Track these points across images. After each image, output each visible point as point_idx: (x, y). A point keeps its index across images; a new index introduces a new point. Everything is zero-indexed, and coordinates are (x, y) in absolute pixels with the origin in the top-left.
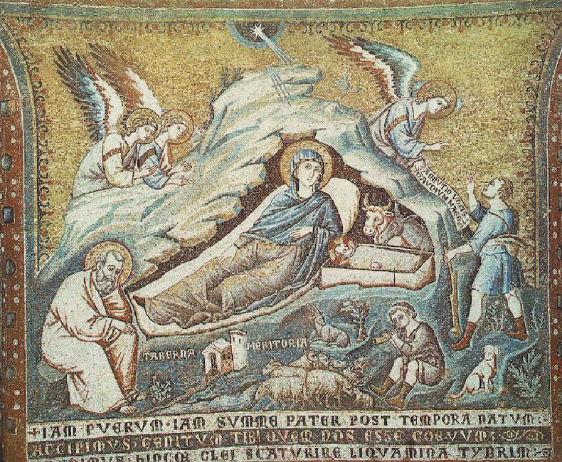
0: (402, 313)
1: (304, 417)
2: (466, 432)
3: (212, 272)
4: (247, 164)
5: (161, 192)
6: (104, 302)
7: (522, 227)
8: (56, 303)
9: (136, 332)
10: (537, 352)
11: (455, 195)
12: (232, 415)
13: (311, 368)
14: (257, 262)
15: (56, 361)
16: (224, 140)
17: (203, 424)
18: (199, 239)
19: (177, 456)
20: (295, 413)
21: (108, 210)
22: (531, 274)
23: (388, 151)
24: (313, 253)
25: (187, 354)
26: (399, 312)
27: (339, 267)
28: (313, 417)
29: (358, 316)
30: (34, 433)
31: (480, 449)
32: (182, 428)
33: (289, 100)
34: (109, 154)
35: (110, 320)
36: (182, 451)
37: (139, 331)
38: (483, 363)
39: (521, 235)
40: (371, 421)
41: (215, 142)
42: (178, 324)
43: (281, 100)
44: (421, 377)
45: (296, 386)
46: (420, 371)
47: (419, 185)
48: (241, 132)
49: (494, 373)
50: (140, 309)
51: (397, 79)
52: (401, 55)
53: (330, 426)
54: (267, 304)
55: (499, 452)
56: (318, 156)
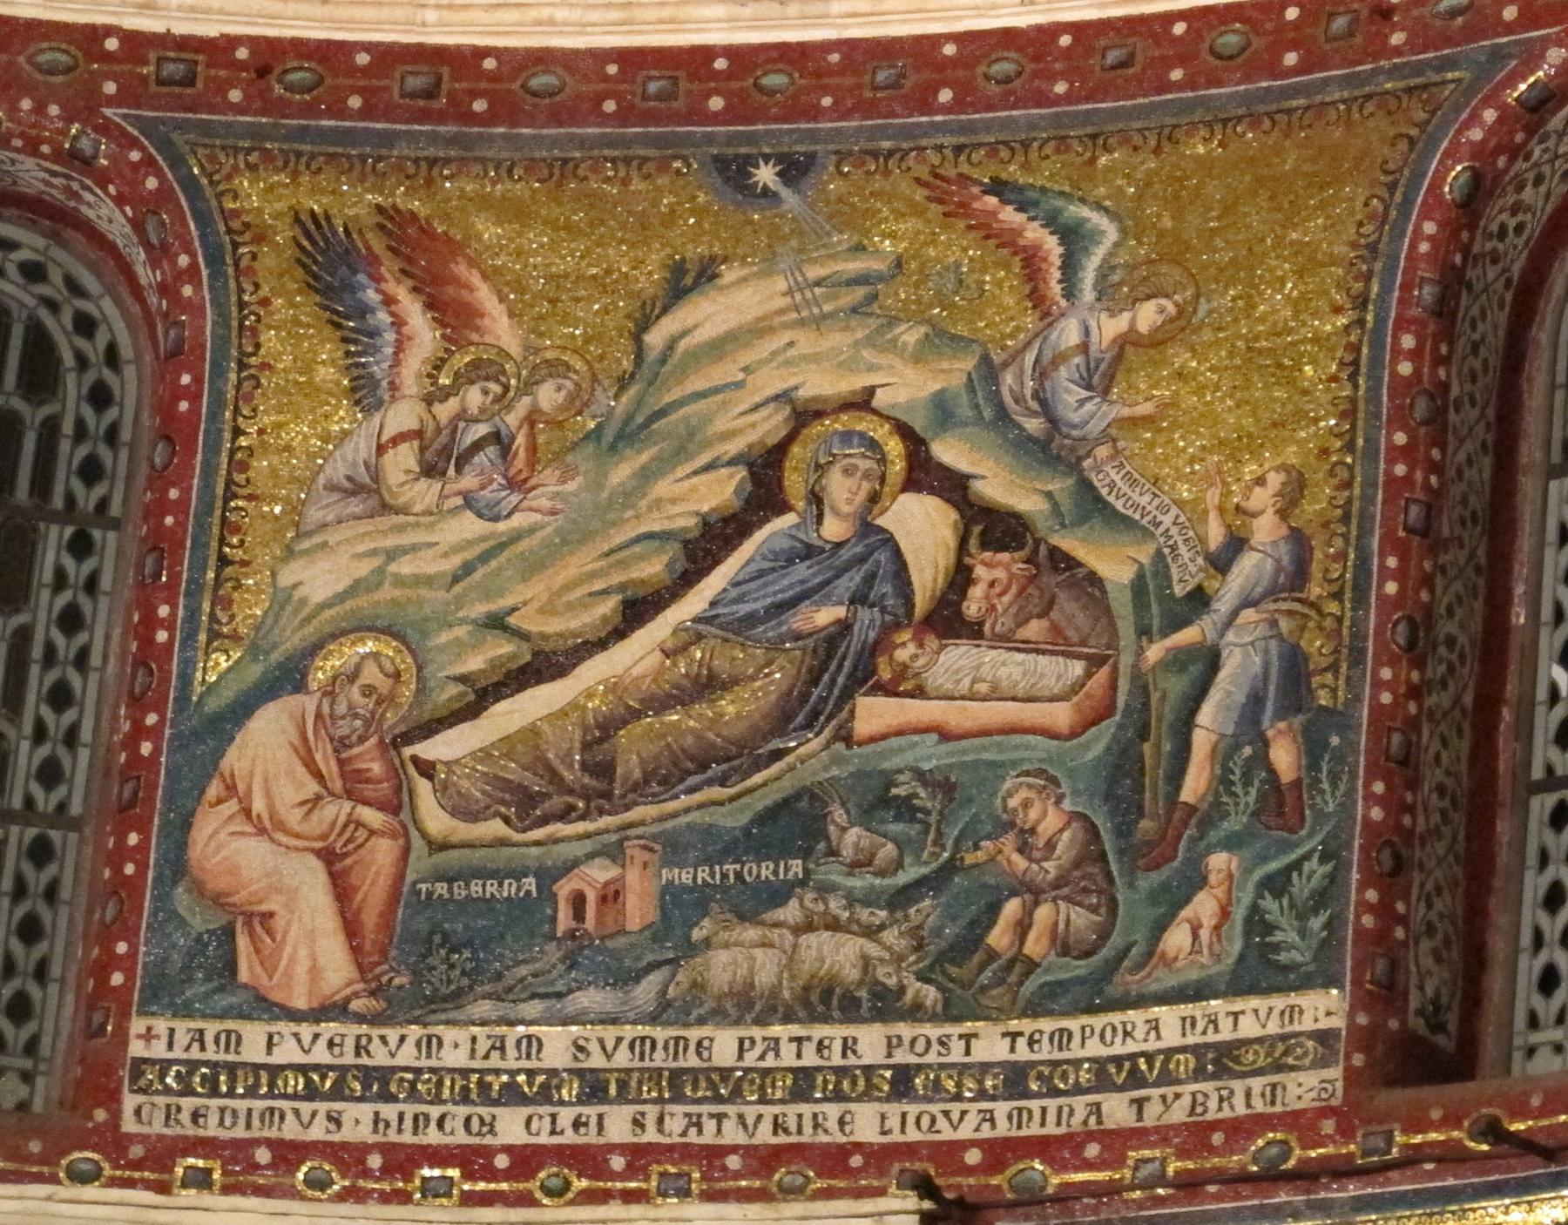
0: (1032, 794)
1: (777, 1040)
2: (1149, 1057)
4: (709, 467)
5: (502, 526)
6: (341, 763)
8: (235, 759)
9: (406, 834)
10: (1323, 859)
12: (610, 1033)
13: (808, 927)
14: (707, 685)
15: (217, 883)
16: (662, 413)
17: (539, 1051)
18: (576, 636)
19: (468, 1120)
20: (757, 1032)
21: (376, 562)
22: (1329, 678)
23: (1034, 425)
24: (840, 666)
25: (519, 889)
26: (1024, 794)
27: (897, 695)
28: (799, 1040)
30: (148, 1036)
31: (1177, 1096)
32: (486, 1057)
33: (819, 322)
34: (396, 440)
35: (347, 806)
36: (483, 1111)
37: (414, 833)
38: (1201, 896)
39: (1315, 590)
40: (935, 1047)
41: (640, 419)
42: (507, 821)
43: (802, 323)
44: (1063, 945)
45: (766, 969)
46: (1061, 926)
47: (1098, 499)
49: (1225, 913)
50: (423, 786)
51: (1070, 266)
52: (1086, 212)
53: (837, 1060)
54: (723, 781)
55: (1221, 1099)
56: (873, 445)
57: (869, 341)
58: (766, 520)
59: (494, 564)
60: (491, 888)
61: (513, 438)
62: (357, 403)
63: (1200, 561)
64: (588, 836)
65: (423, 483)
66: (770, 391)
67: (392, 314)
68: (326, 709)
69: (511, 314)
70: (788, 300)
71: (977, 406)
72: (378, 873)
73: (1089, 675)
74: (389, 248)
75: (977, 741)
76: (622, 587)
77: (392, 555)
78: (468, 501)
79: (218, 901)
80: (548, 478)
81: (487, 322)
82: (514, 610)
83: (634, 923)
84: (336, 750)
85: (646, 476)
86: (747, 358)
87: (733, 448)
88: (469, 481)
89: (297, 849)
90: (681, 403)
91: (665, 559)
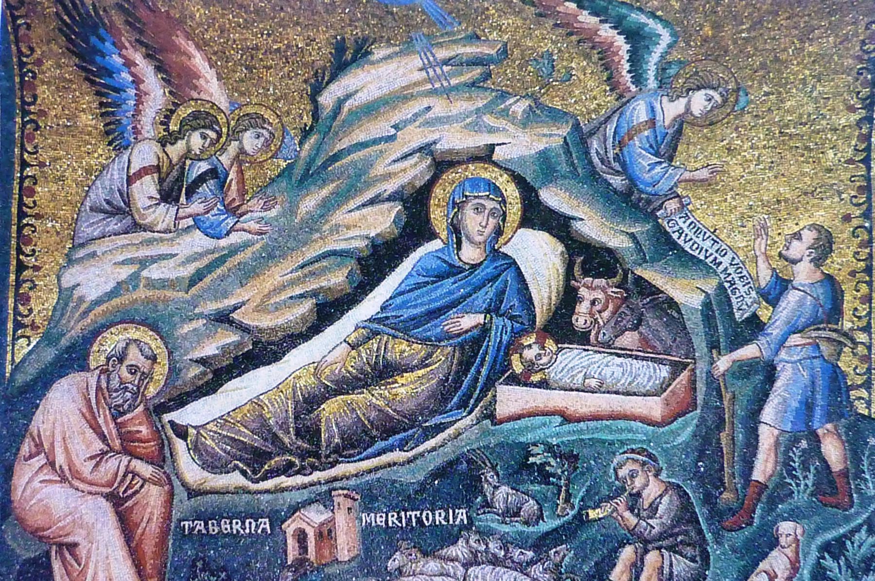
0: (636, 467)
3: (307, 381)
4: (372, 202)
5: (223, 242)
7: (848, 313)
11: (733, 258)
15: (35, 520)
16: (336, 158)
24: (483, 360)
25: (257, 527)
29: (559, 471)
33: (447, 92)
35: (125, 459)
37: (176, 483)
42: (244, 473)
46: (666, 570)
48: (363, 145)
50: (180, 445)
51: (636, 60)
56: (496, 190)
57: (488, 109)
58: (418, 245)
59: (219, 271)
60: (237, 526)
61: (227, 175)
62: (110, 144)
63: (753, 294)
64: (304, 487)
65: (163, 207)
66: (415, 145)
67: (133, 74)
68: (104, 385)
69: (219, 79)
70: (424, 74)
71: (573, 164)
72: (152, 513)
73: (674, 375)
74: (127, 22)
75: (592, 424)
76: (314, 294)
77: (144, 263)
78: (198, 223)
79: (36, 534)
80: (256, 204)
81: (202, 81)
82: (235, 308)
83: (344, 555)
84: (114, 419)
85: (327, 207)
86: (397, 117)
87: (390, 187)
88: (196, 207)
89: (90, 493)
90: (349, 150)
91: (346, 272)
